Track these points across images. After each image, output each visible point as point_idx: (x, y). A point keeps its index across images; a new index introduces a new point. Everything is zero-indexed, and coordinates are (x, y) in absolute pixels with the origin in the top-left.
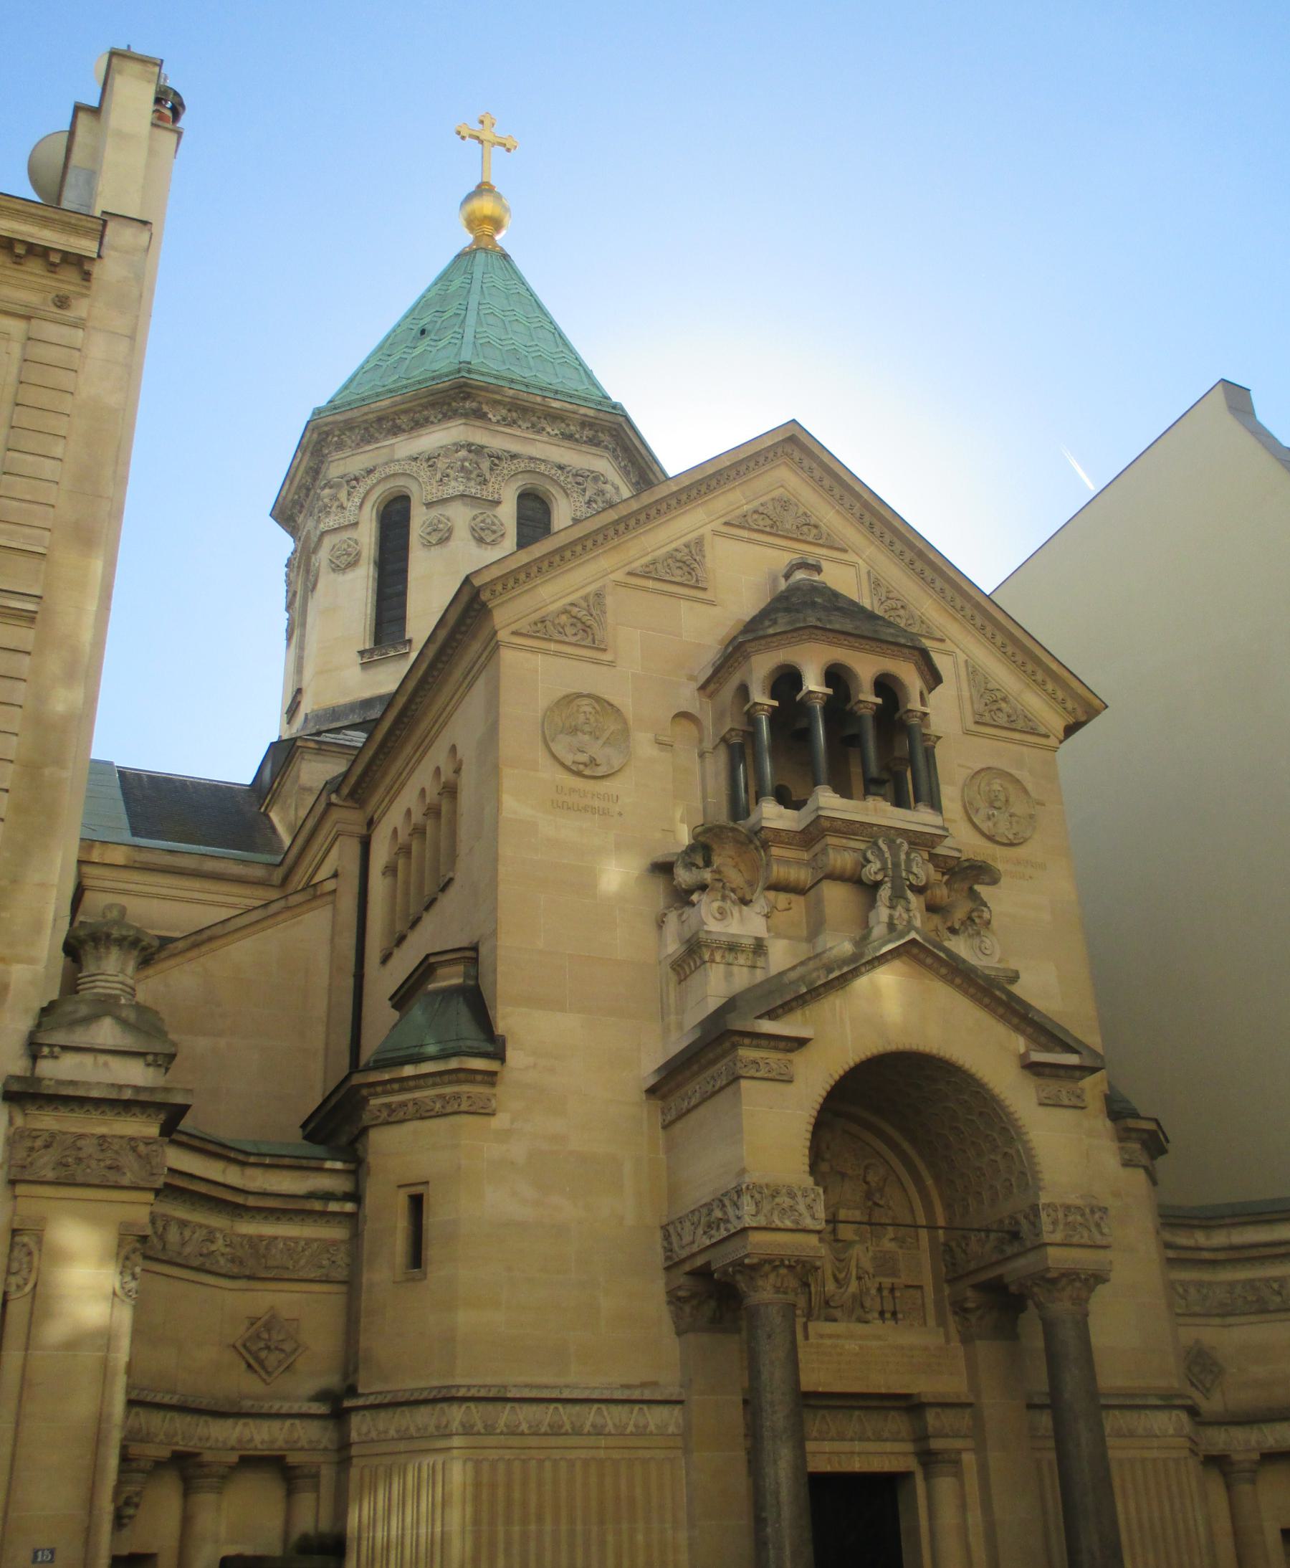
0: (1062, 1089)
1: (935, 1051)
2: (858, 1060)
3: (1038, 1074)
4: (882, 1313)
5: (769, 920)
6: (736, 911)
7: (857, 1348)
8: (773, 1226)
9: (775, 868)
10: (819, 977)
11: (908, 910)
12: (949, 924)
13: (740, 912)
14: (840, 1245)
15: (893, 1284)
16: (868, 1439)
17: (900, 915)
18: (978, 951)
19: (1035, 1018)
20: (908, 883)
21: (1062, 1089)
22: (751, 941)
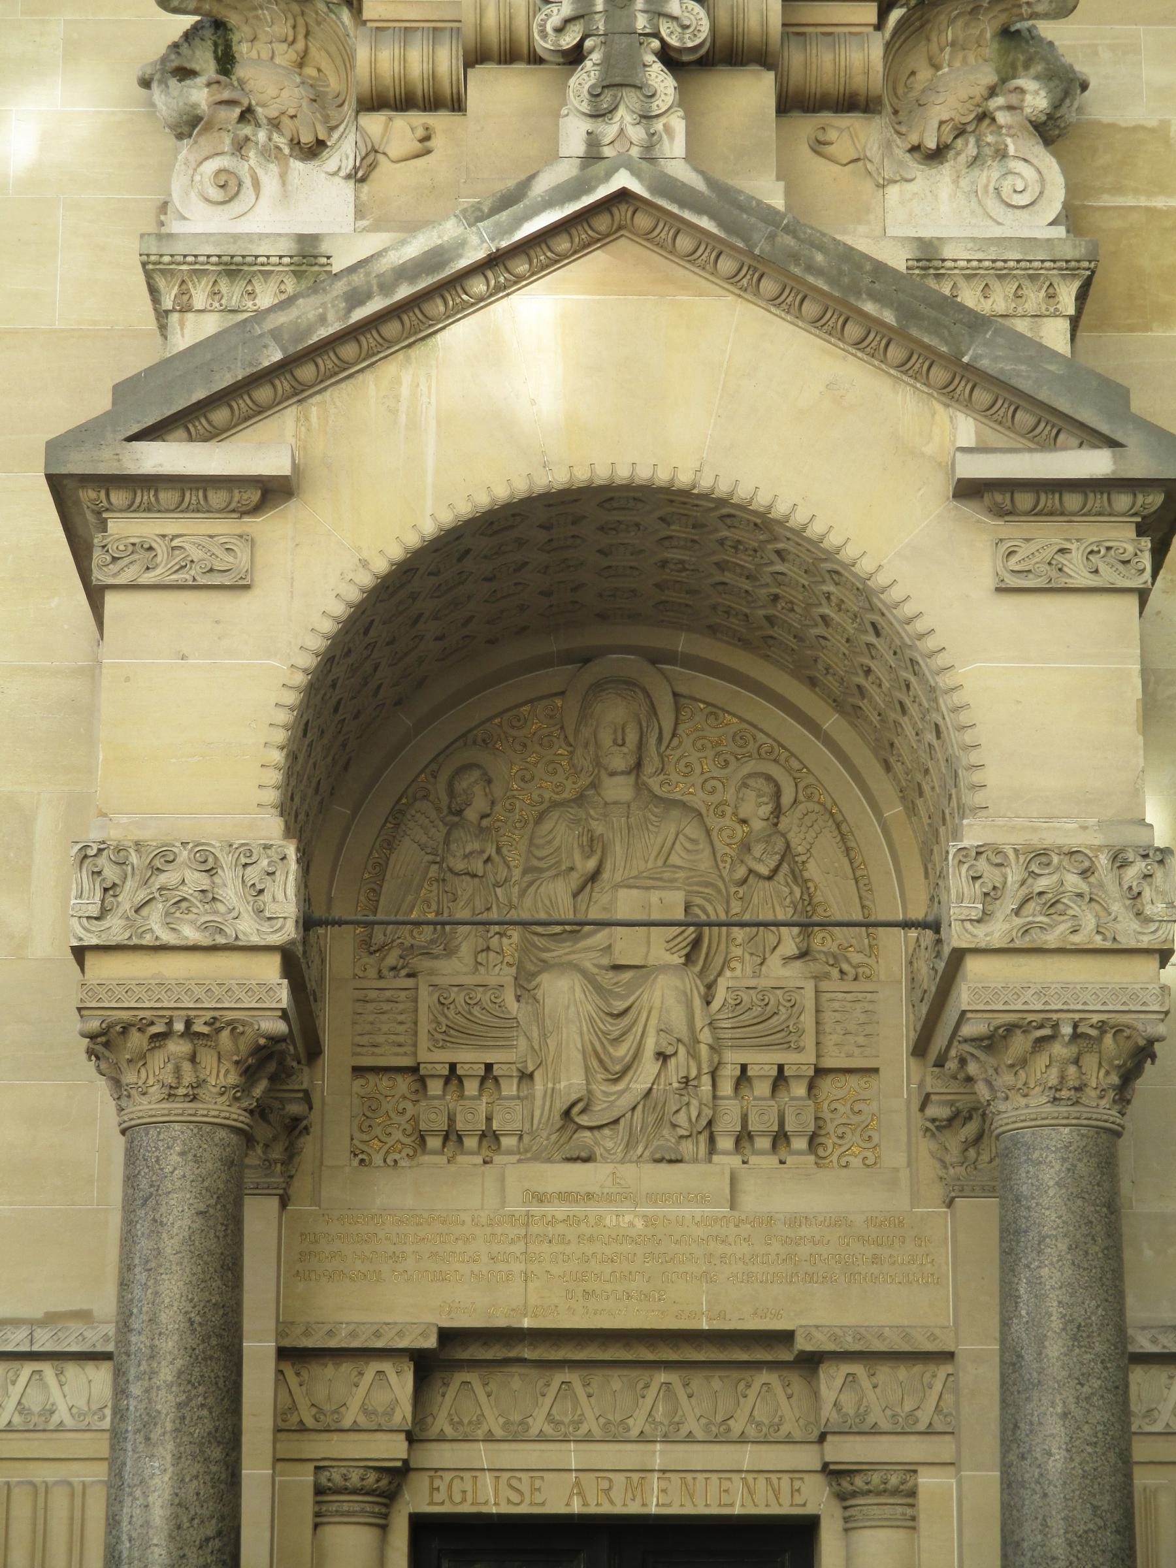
0: (1073, 546)
1: (684, 479)
2: (447, 518)
3: (1001, 512)
4: (780, 1138)
5: (365, 188)
6: (269, 178)
7: (639, 1224)
8: (148, 940)
9: (362, 54)
10: (322, 319)
11: (646, 117)
12: (914, 139)
13: (283, 177)
14: (627, 975)
15: (781, 1068)
16: (690, 1439)
17: (622, 131)
18: (992, 204)
19: (985, 364)
20: (656, 44)
21: (1073, 546)
22: (285, 247)
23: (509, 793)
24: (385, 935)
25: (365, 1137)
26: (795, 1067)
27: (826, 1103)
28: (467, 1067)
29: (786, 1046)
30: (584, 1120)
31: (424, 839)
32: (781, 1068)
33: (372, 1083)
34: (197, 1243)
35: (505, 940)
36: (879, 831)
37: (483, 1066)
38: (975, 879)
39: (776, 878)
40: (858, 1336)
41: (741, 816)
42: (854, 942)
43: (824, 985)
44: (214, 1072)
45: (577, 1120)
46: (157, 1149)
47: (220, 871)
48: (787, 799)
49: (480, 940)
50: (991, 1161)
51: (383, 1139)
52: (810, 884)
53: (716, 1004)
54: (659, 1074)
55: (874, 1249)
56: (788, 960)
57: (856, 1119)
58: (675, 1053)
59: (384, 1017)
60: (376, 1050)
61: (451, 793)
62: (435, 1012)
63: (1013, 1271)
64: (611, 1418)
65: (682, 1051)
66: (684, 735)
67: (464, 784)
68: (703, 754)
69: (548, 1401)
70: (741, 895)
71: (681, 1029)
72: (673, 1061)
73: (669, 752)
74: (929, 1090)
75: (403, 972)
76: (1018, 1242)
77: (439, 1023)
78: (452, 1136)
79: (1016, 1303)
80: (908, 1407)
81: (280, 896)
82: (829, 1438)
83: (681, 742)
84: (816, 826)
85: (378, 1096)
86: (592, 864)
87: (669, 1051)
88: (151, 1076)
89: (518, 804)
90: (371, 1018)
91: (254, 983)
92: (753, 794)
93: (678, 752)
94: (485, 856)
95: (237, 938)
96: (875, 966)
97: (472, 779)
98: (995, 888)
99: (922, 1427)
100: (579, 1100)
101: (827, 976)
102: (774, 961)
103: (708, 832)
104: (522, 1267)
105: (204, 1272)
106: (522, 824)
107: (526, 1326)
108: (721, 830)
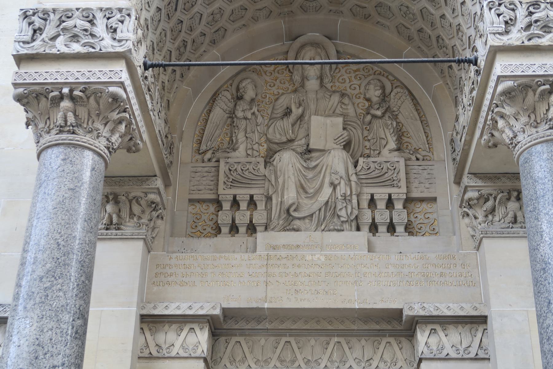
7: (323, 258)
8: (54, 51)
15: (390, 195)
23: (264, 91)
24: (207, 147)
25: (193, 231)
26: (397, 195)
27: (412, 214)
28: (241, 196)
29: (393, 186)
30: (296, 214)
31: (226, 107)
32: (390, 195)
33: (198, 208)
34: (67, 204)
35: (261, 147)
36: (431, 100)
37: (249, 196)
38: (499, 15)
39: (384, 118)
40: (437, 308)
41: (367, 96)
42: (421, 146)
43: (409, 163)
44: (86, 121)
45: (292, 214)
46: (51, 158)
47: (95, 21)
48: (388, 90)
49: (249, 145)
50: (499, 221)
51: (202, 232)
52: (400, 124)
53: (359, 168)
54: (331, 194)
55: (441, 270)
56: (391, 151)
57: (426, 221)
58: (340, 183)
59: (204, 178)
60: (199, 192)
61: (238, 89)
62: (227, 173)
63: (538, 219)
64: (310, 359)
65: (343, 182)
66: (341, 68)
67: (244, 84)
68: (350, 75)
69: (278, 351)
70: (368, 129)
71: (342, 172)
72: (338, 187)
73: (334, 74)
74: (467, 184)
75: (214, 160)
76: (539, 203)
77: (229, 178)
78: (234, 229)
79: (541, 235)
80: (464, 345)
81: (125, 30)
82: (423, 361)
83: (340, 71)
84: (402, 99)
85: (201, 213)
86: (300, 110)
87: (336, 182)
88: (52, 123)
89: (268, 95)
90: (198, 179)
91: (108, 70)
92: (373, 86)
93: (339, 75)
94: (252, 111)
95: (101, 50)
96: (432, 156)
97: (247, 82)
98: (511, 19)
99: (472, 355)
100: (294, 204)
101: (410, 159)
102: (385, 152)
103: (353, 104)
104: (265, 279)
105: (69, 219)
106: (269, 103)
107: (266, 307)
108: (358, 104)
